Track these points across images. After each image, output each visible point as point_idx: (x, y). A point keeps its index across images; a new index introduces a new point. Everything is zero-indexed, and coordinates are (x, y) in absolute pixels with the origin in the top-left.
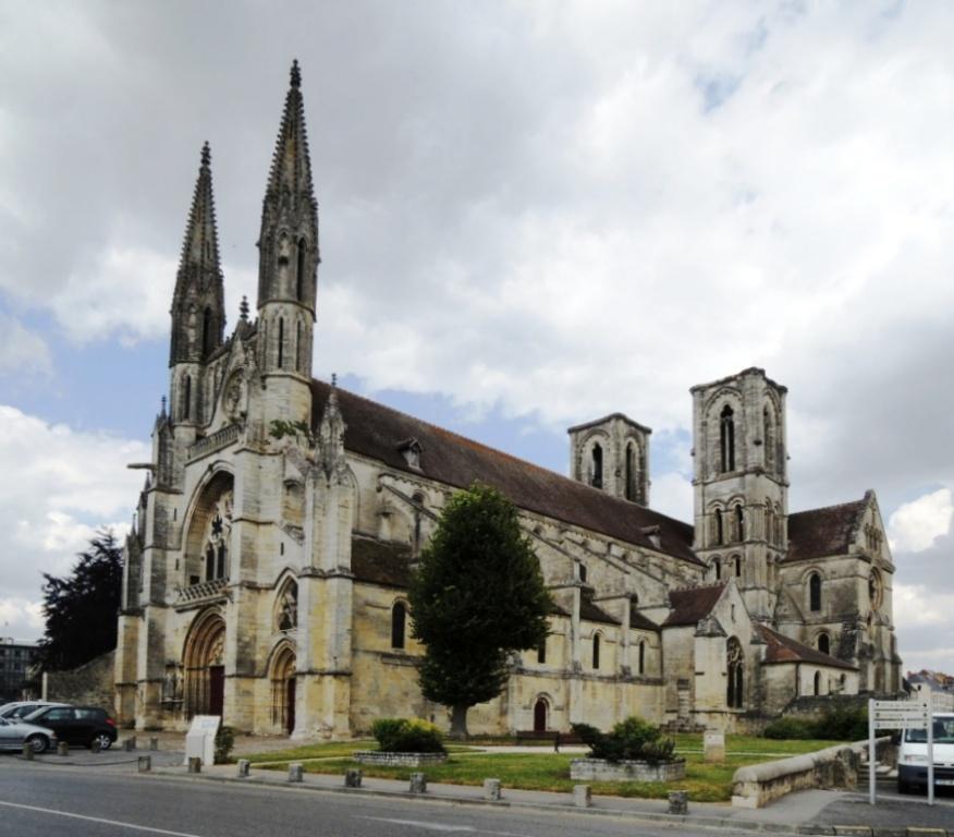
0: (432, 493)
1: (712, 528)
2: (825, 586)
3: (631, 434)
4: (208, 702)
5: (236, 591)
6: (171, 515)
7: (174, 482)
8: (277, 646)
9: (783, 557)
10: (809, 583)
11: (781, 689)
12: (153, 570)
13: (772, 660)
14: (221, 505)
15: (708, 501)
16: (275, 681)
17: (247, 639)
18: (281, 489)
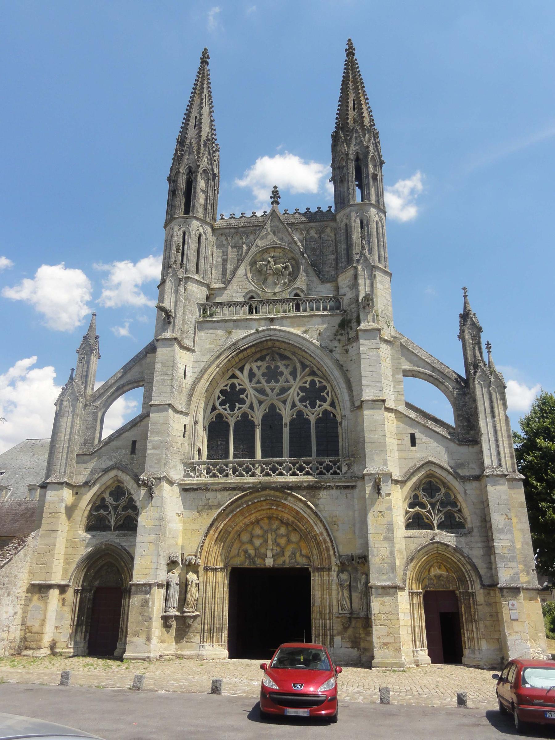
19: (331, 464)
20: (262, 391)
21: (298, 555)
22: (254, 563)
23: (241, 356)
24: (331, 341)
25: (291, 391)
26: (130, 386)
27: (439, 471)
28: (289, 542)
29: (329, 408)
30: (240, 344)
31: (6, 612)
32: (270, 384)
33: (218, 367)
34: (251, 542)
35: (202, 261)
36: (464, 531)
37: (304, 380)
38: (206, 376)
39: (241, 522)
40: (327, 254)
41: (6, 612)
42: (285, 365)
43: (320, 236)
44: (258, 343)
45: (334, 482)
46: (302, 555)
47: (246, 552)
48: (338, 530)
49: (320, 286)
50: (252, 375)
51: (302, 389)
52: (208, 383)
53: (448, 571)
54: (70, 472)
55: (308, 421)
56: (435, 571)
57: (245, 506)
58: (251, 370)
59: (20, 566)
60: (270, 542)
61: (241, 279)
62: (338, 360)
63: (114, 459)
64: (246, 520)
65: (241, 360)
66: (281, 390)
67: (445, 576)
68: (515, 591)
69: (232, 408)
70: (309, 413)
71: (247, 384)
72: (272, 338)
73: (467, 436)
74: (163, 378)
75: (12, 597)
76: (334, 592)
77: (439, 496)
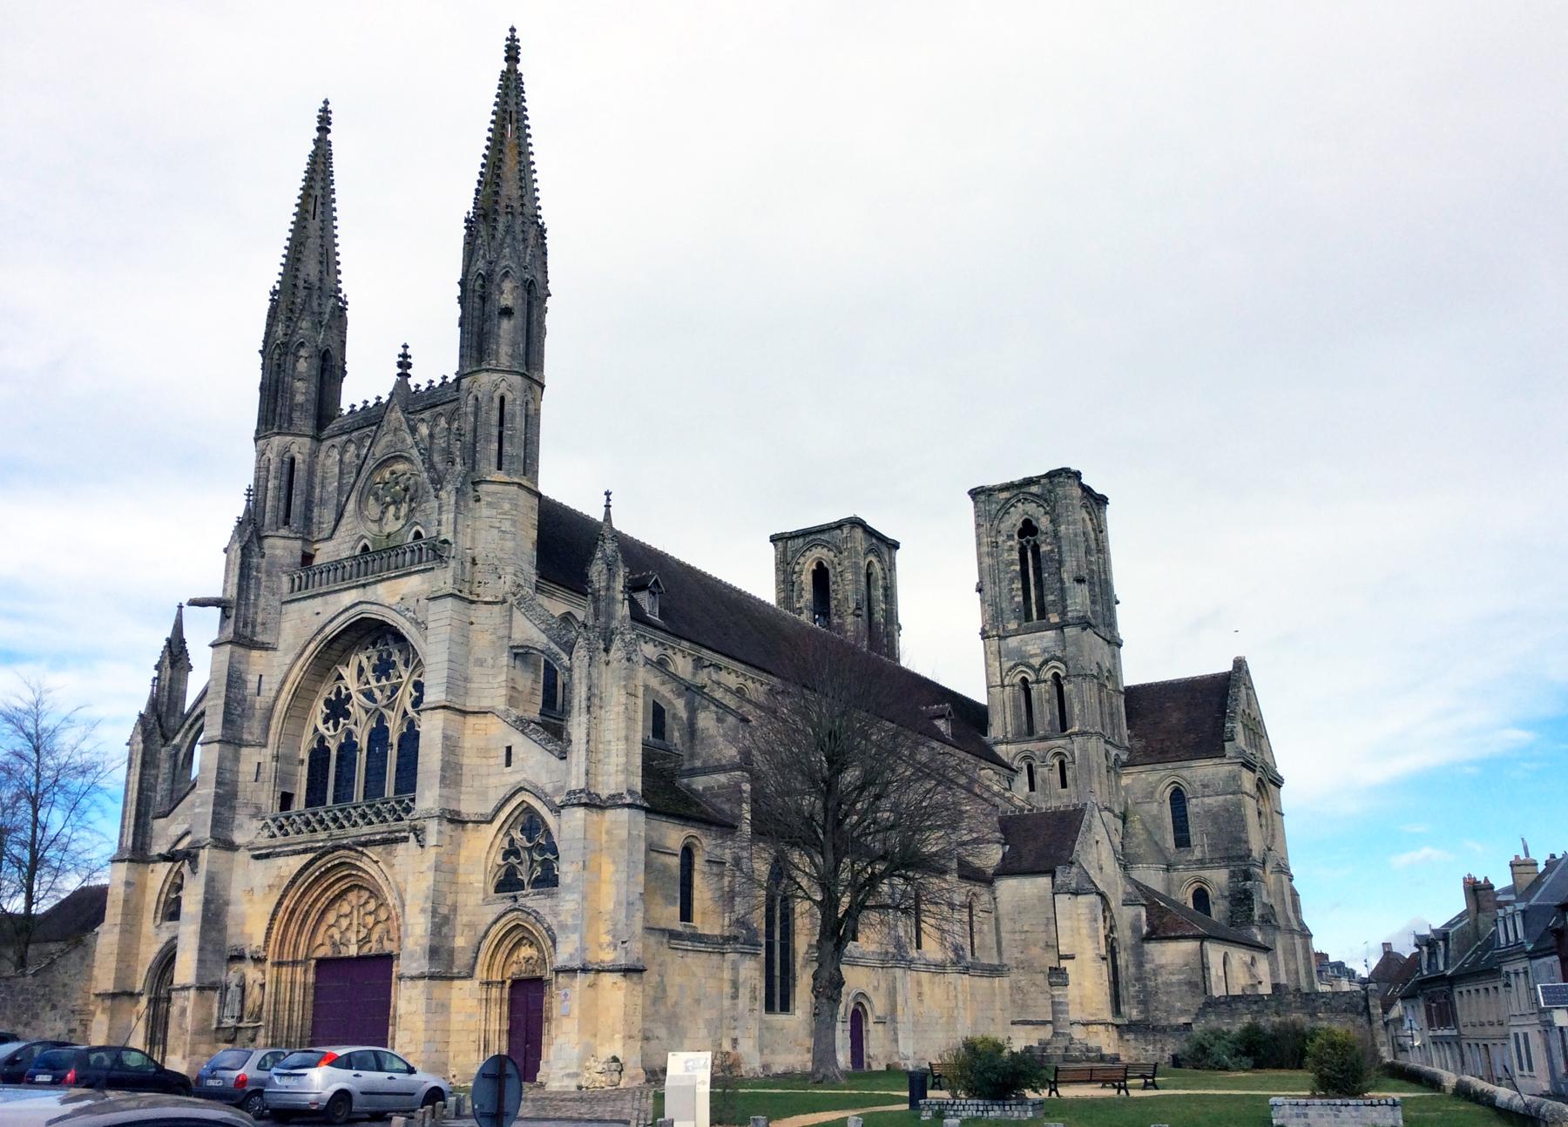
0: (679, 659)
1: (1016, 707)
2: (1193, 806)
3: (870, 551)
4: (309, 1024)
5: (432, 827)
7: (259, 629)
8: (495, 922)
9: (1124, 757)
10: (1168, 801)
11: (1180, 983)
12: (219, 783)
13: (1157, 933)
14: (349, 673)
15: (1008, 665)
16: (488, 984)
17: (444, 910)
18: (505, 659)
50: (361, 670)
52: (290, 697)
60: (355, 922)
61: (350, 520)
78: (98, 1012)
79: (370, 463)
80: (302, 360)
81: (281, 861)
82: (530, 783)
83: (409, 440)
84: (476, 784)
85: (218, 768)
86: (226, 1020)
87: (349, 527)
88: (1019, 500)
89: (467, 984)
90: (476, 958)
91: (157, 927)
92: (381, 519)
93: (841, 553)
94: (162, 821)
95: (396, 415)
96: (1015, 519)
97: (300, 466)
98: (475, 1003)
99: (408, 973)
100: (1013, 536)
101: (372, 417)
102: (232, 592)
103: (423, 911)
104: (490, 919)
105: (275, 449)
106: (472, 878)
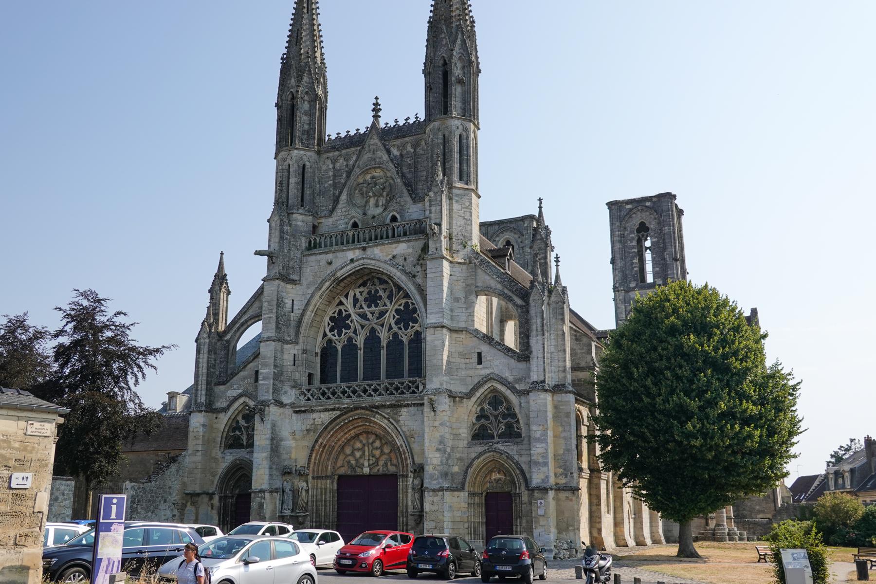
6: (289, 306)
8: (477, 458)
16: (472, 494)
19: (410, 384)
20: (363, 316)
21: (389, 464)
22: (355, 472)
23: (342, 284)
24: (415, 266)
25: (387, 314)
26: (253, 321)
27: (499, 387)
28: (382, 453)
29: (419, 329)
30: (339, 274)
31: (165, 515)
32: (370, 309)
33: (320, 298)
34: (352, 454)
35: (307, 192)
36: (518, 440)
37: (399, 303)
38: (311, 308)
39: (342, 437)
40: (422, 170)
41: (165, 515)
42: (383, 289)
43: (415, 152)
44: (354, 272)
45: (411, 400)
46: (392, 465)
47: (349, 462)
48: (414, 442)
49: (413, 206)
50: (356, 301)
51: (397, 311)
52: (313, 314)
53: (505, 475)
54: (209, 401)
55: (402, 341)
56: (495, 476)
57: (342, 424)
58: (355, 295)
59: (174, 480)
60: (367, 453)
62: (420, 285)
63: (242, 388)
64: (347, 435)
65: (344, 287)
66: (380, 314)
67: (503, 480)
68: (544, 490)
69: (340, 335)
70: (402, 334)
71: (351, 311)
72: (365, 266)
73: (526, 352)
74: (269, 315)
75: (168, 504)
76: (410, 495)
77: (502, 409)
78: (189, 504)
79: (357, 171)
80: (306, 103)
81: (315, 415)
82: (497, 375)
83: (385, 157)
84: (459, 374)
85: (275, 357)
86: (285, 511)
87: (343, 210)
88: (639, 210)
89: (462, 494)
90: (465, 479)
91: (222, 453)
92: (365, 206)
93: (523, 235)
94: (222, 387)
95: (375, 141)
96: (636, 221)
97: (308, 170)
98: (466, 505)
99: (430, 487)
100: (634, 231)
101: (355, 141)
102: (275, 246)
103: (438, 450)
104: (473, 456)
105: (294, 158)
106: (461, 431)
